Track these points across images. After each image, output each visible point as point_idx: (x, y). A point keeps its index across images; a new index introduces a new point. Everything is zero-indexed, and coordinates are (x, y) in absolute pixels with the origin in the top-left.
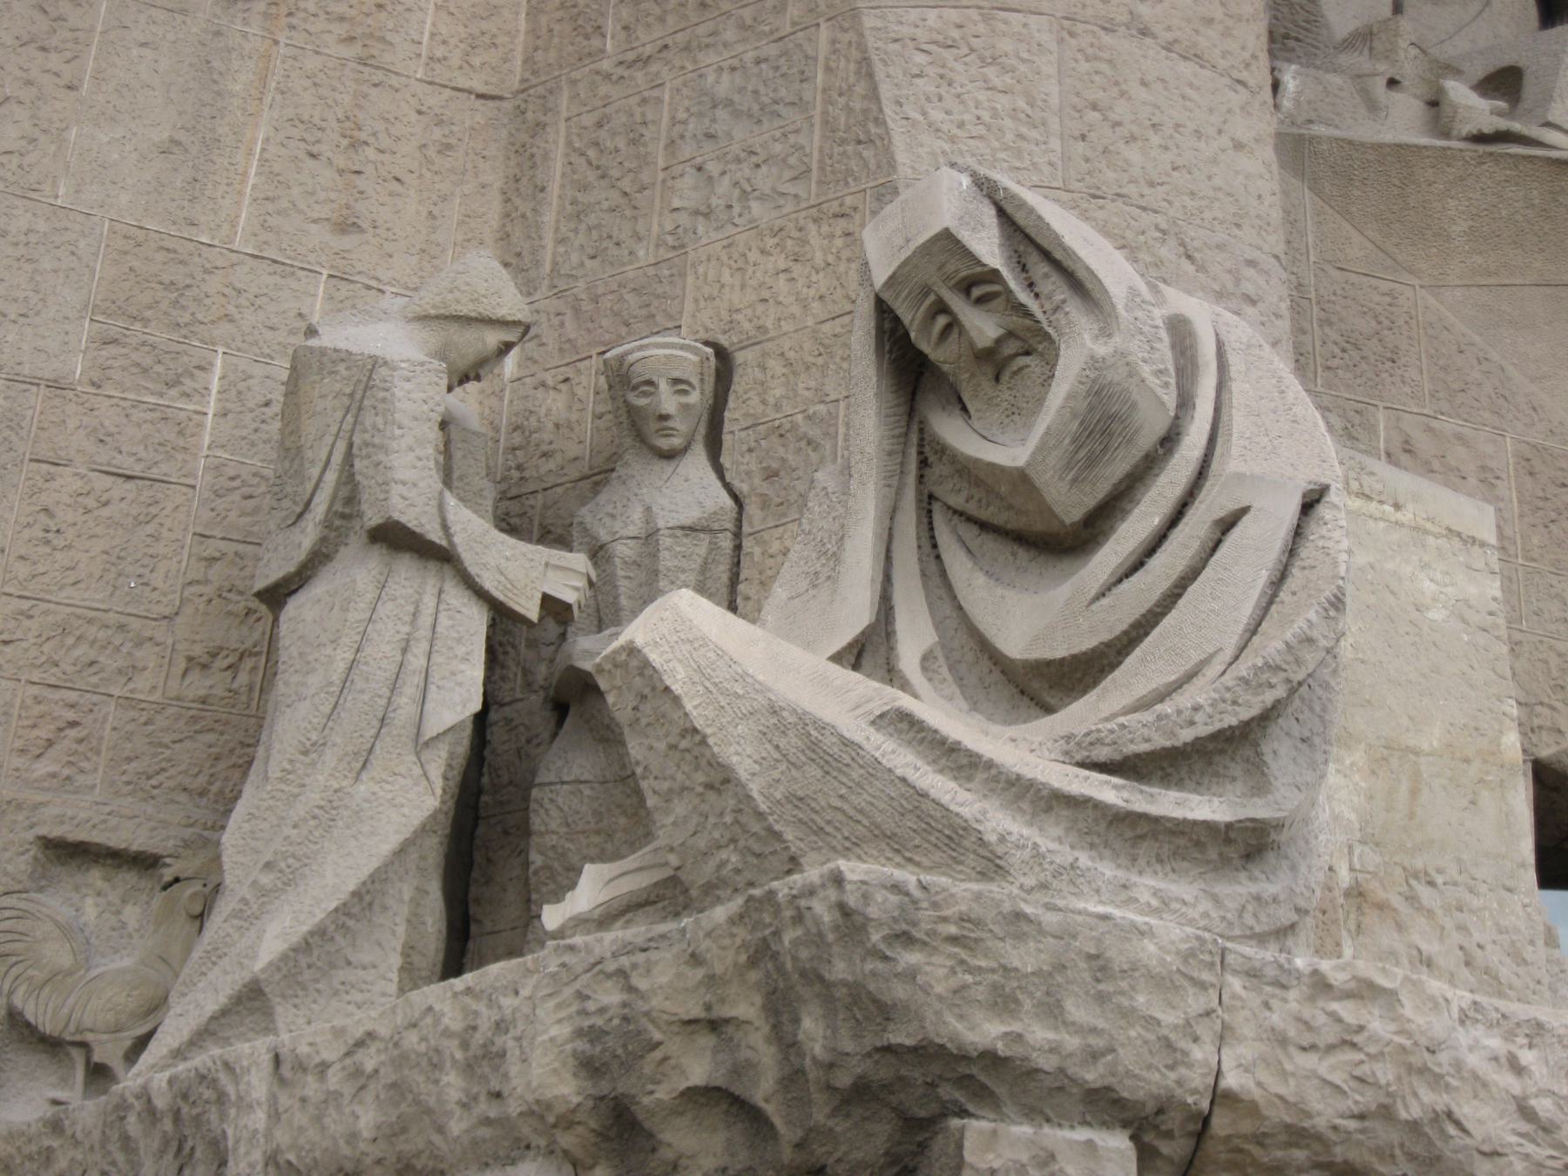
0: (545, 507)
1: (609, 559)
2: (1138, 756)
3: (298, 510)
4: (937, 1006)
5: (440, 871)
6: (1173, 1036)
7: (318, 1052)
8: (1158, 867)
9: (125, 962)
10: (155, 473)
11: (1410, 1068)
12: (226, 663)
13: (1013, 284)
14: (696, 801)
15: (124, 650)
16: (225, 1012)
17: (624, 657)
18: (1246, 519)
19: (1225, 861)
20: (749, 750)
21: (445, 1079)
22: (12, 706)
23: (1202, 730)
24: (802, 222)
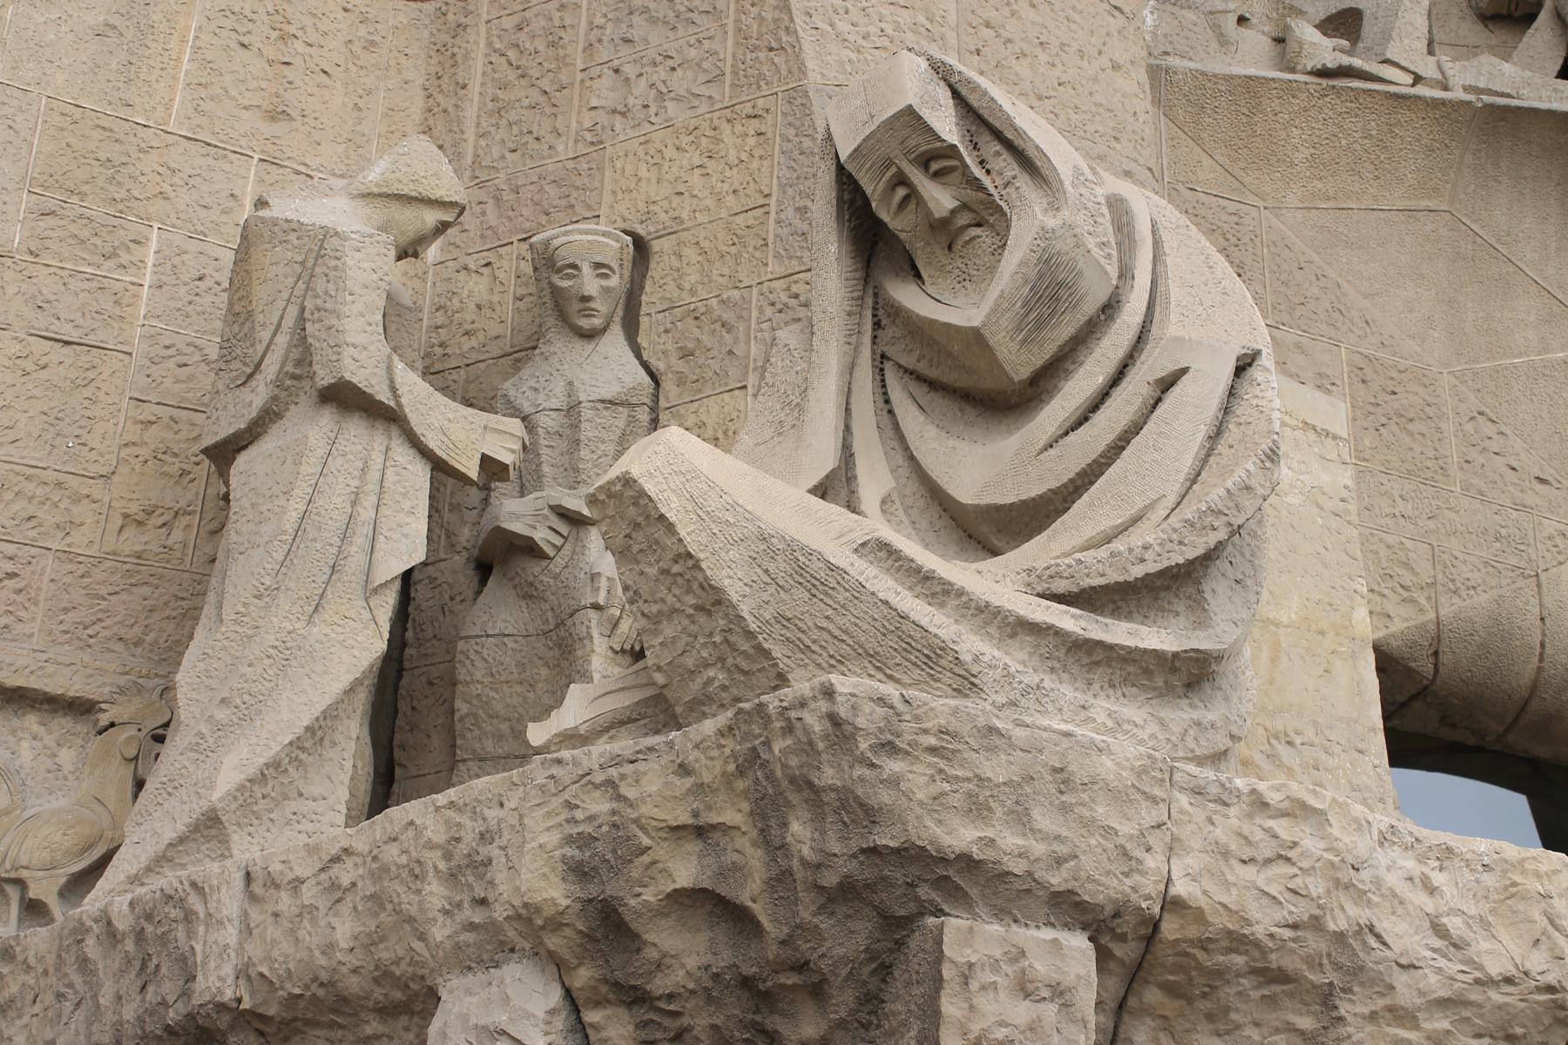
0: (467, 381)
2: (1093, 588)
3: (249, 371)
4: (919, 811)
6: (1128, 846)
7: (291, 869)
8: (1111, 691)
11: (1337, 882)
12: (161, 521)
13: (968, 160)
14: (686, 622)
16: (182, 840)
17: (618, 487)
21: (428, 888)
23: (1152, 568)
24: (716, 122)
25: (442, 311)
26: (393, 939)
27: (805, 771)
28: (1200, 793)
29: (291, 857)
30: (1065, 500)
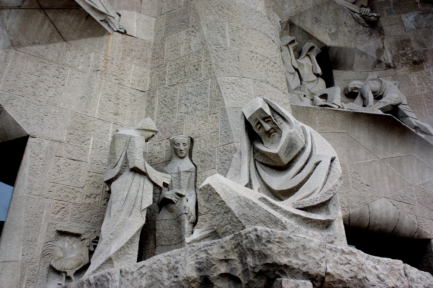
2: (307, 207)
3: (115, 165)
4: (276, 255)
6: (318, 262)
8: (311, 229)
9: (74, 255)
10: (79, 159)
11: (359, 268)
14: (222, 215)
15: (74, 193)
16: (104, 263)
17: (207, 187)
20: (234, 205)
21: (163, 274)
23: (319, 202)
25: (150, 154)
26: (155, 285)
27: (251, 247)
29: (131, 267)
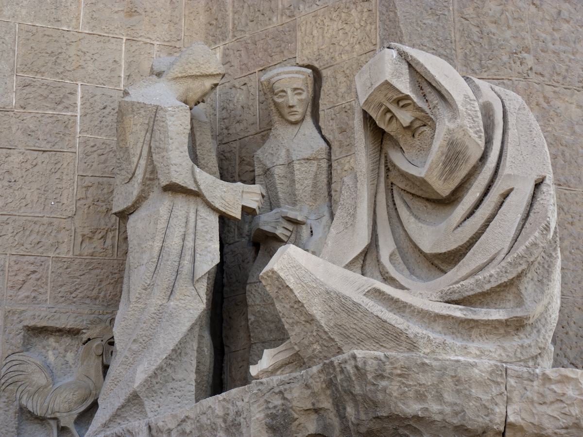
0: (241, 148)
1: (272, 176)
3: (130, 177)
5: (209, 325)
6: (487, 404)
7: (166, 425)
8: (480, 338)
9: (69, 379)
10: (56, 148)
12: (100, 236)
13: (415, 100)
14: (303, 327)
16: (123, 406)
18: (512, 193)
19: (507, 333)
22: (5, 267)
23: (494, 284)
25: (225, 110)
28: (520, 378)
30: (467, 249)
